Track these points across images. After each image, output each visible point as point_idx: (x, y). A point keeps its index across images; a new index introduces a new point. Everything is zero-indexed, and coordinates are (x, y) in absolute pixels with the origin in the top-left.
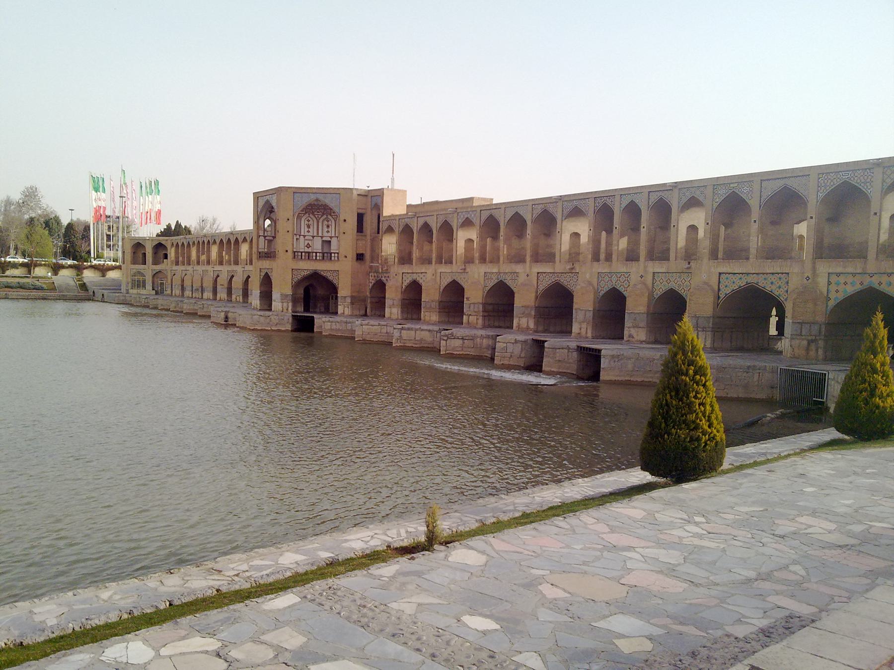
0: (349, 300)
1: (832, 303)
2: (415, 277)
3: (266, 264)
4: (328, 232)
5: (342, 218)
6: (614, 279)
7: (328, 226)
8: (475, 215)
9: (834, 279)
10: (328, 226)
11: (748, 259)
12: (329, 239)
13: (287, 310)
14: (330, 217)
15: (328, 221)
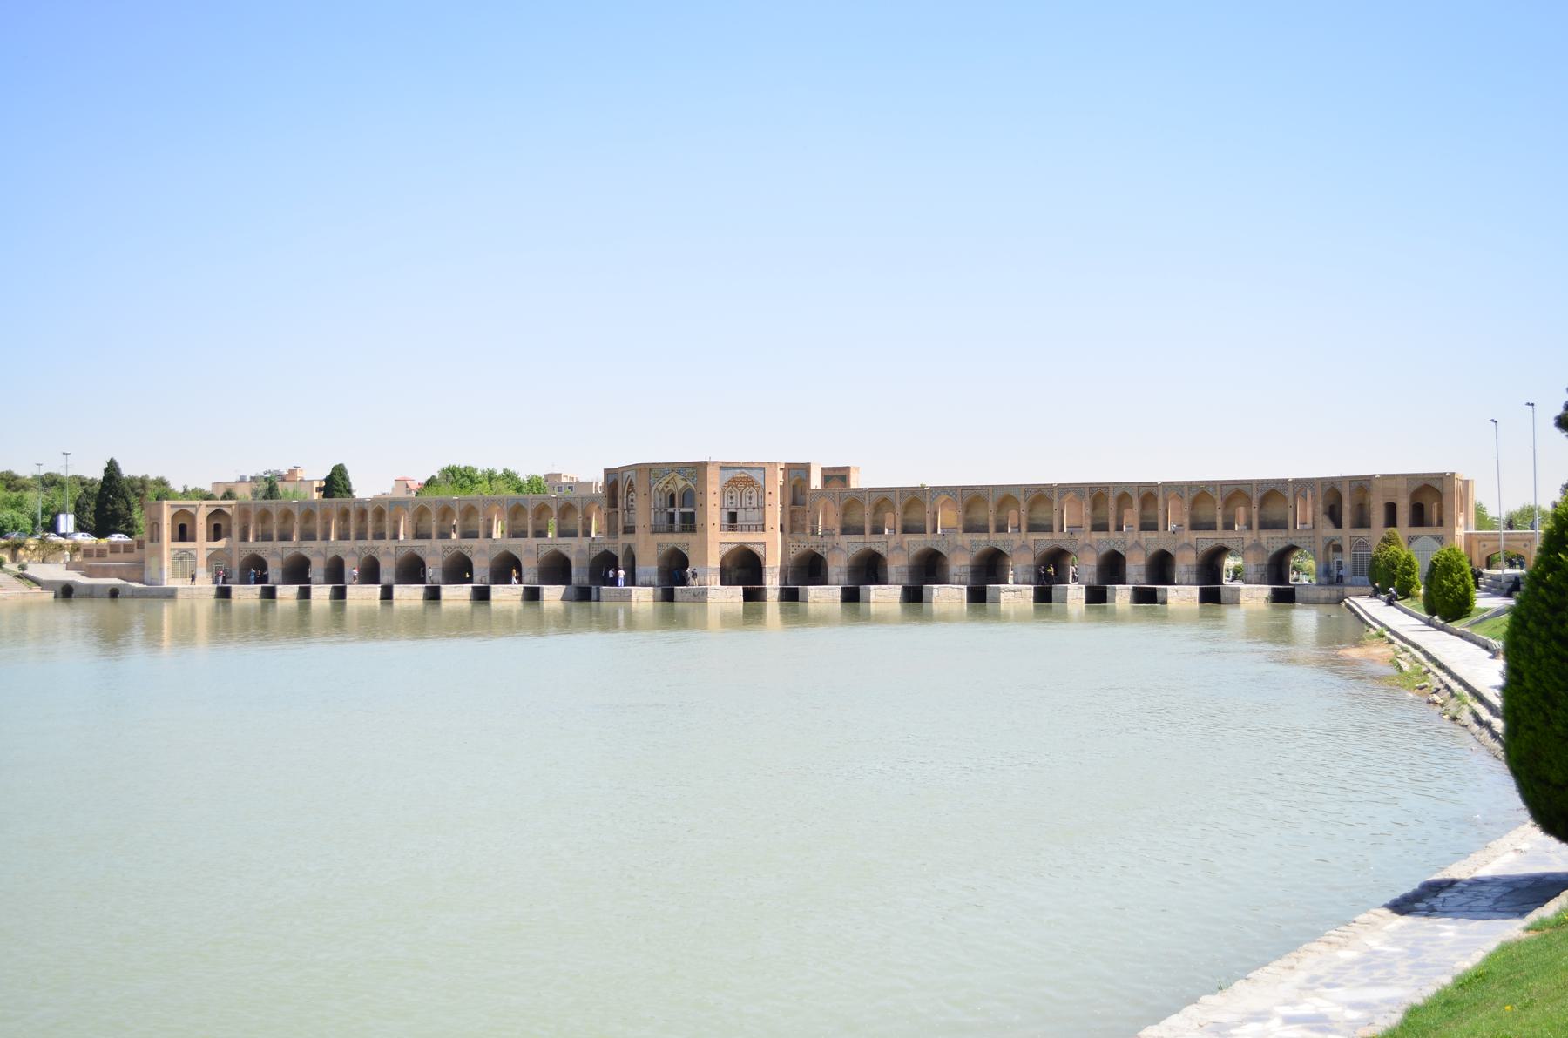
0: (777, 570)
1: (1270, 554)
2: (868, 545)
3: (675, 540)
4: (750, 503)
5: (767, 491)
6: (1112, 544)
7: (731, 498)
8: (954, 494)
9: (1270, 541)
10: (731, 498)
11: (1215, 529)
12: (734, 510)
13: (716, 583)
14: (735, 488)
15: (731, 492)
